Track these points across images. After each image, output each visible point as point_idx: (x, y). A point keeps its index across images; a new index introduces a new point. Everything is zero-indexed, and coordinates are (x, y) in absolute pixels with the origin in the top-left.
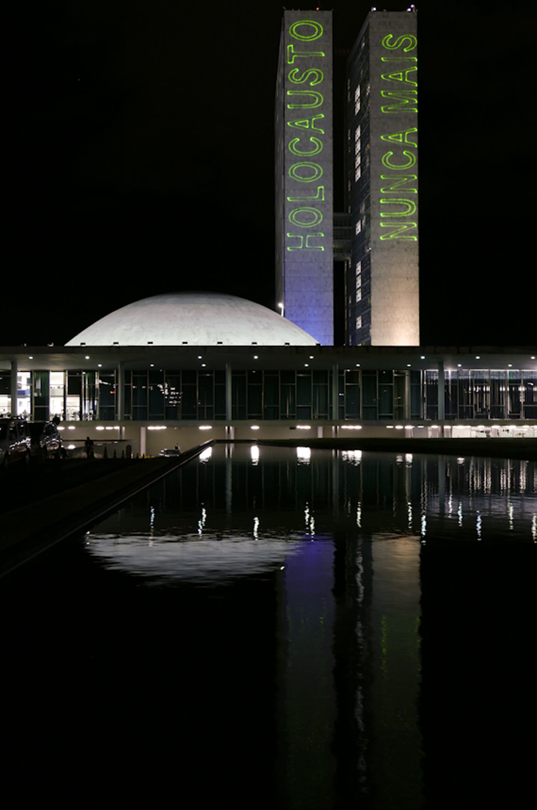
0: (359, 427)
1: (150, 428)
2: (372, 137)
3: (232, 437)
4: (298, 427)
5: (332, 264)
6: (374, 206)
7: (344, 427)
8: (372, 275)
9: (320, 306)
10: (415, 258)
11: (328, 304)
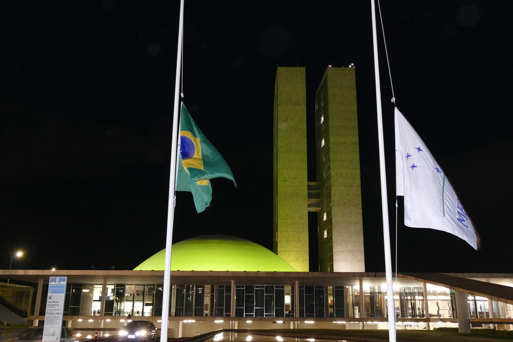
0: (312, 322)
1: (185, 321)
2: (331, 138)
3: (236, 328)
4: (277, 322)
5: (307, 214)
6: (333, 179)
7: (306, 322)
8: (333, 221)
10: (360, 211)
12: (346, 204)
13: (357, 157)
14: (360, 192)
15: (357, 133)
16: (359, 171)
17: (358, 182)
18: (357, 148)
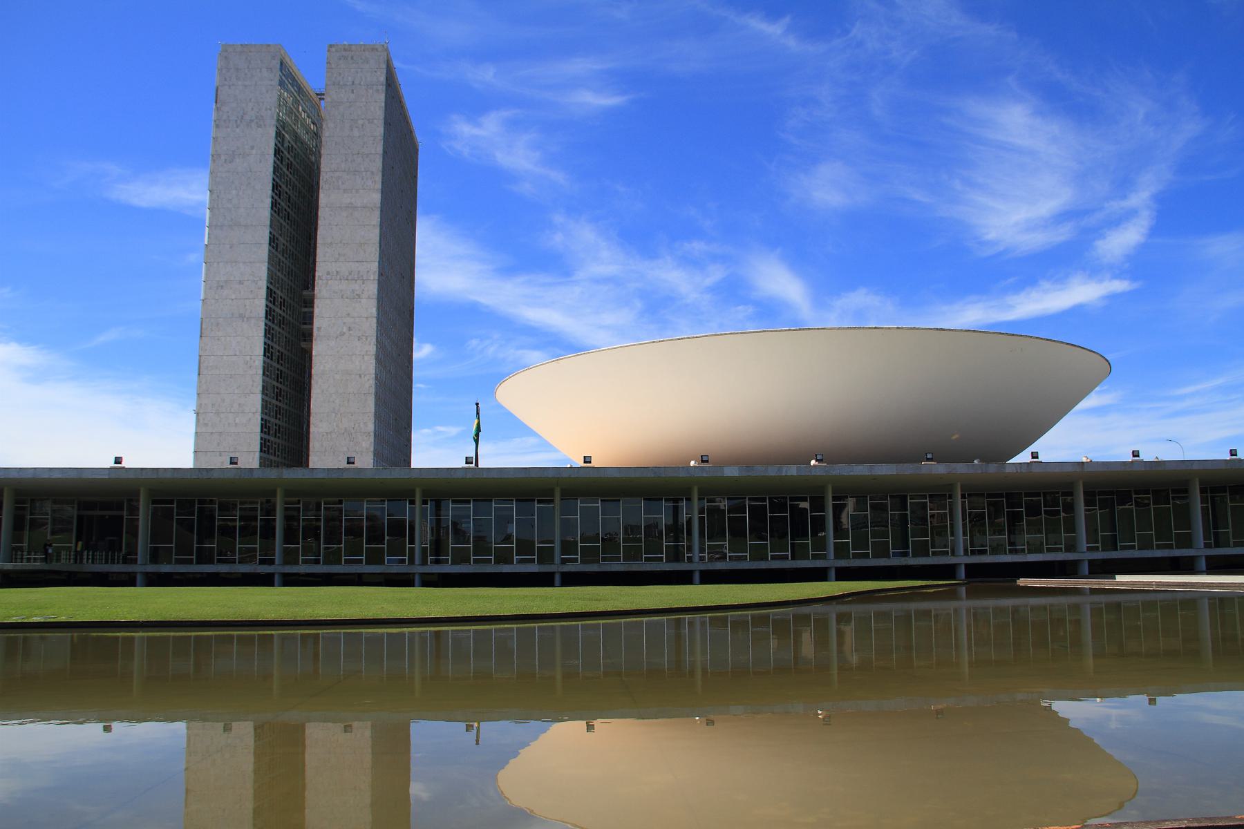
2: (321, 195)
9: (243, 412)
11: (254, 410)
12: (343, 334)
13: (374, 235)
14: (374, 311)
15: (379, 186)
16: (375, 266)
17: (372, 288)
18: (375, 218)
